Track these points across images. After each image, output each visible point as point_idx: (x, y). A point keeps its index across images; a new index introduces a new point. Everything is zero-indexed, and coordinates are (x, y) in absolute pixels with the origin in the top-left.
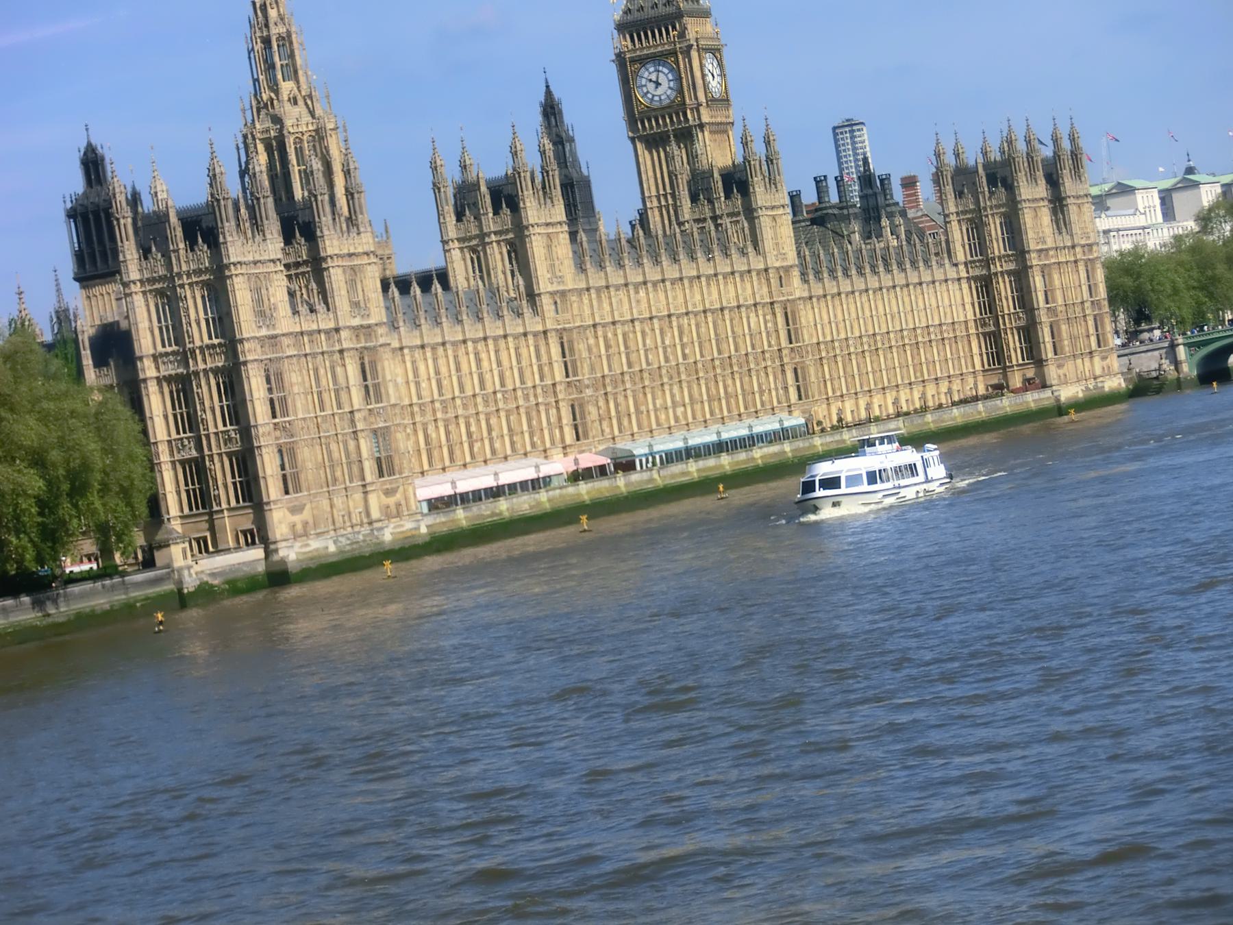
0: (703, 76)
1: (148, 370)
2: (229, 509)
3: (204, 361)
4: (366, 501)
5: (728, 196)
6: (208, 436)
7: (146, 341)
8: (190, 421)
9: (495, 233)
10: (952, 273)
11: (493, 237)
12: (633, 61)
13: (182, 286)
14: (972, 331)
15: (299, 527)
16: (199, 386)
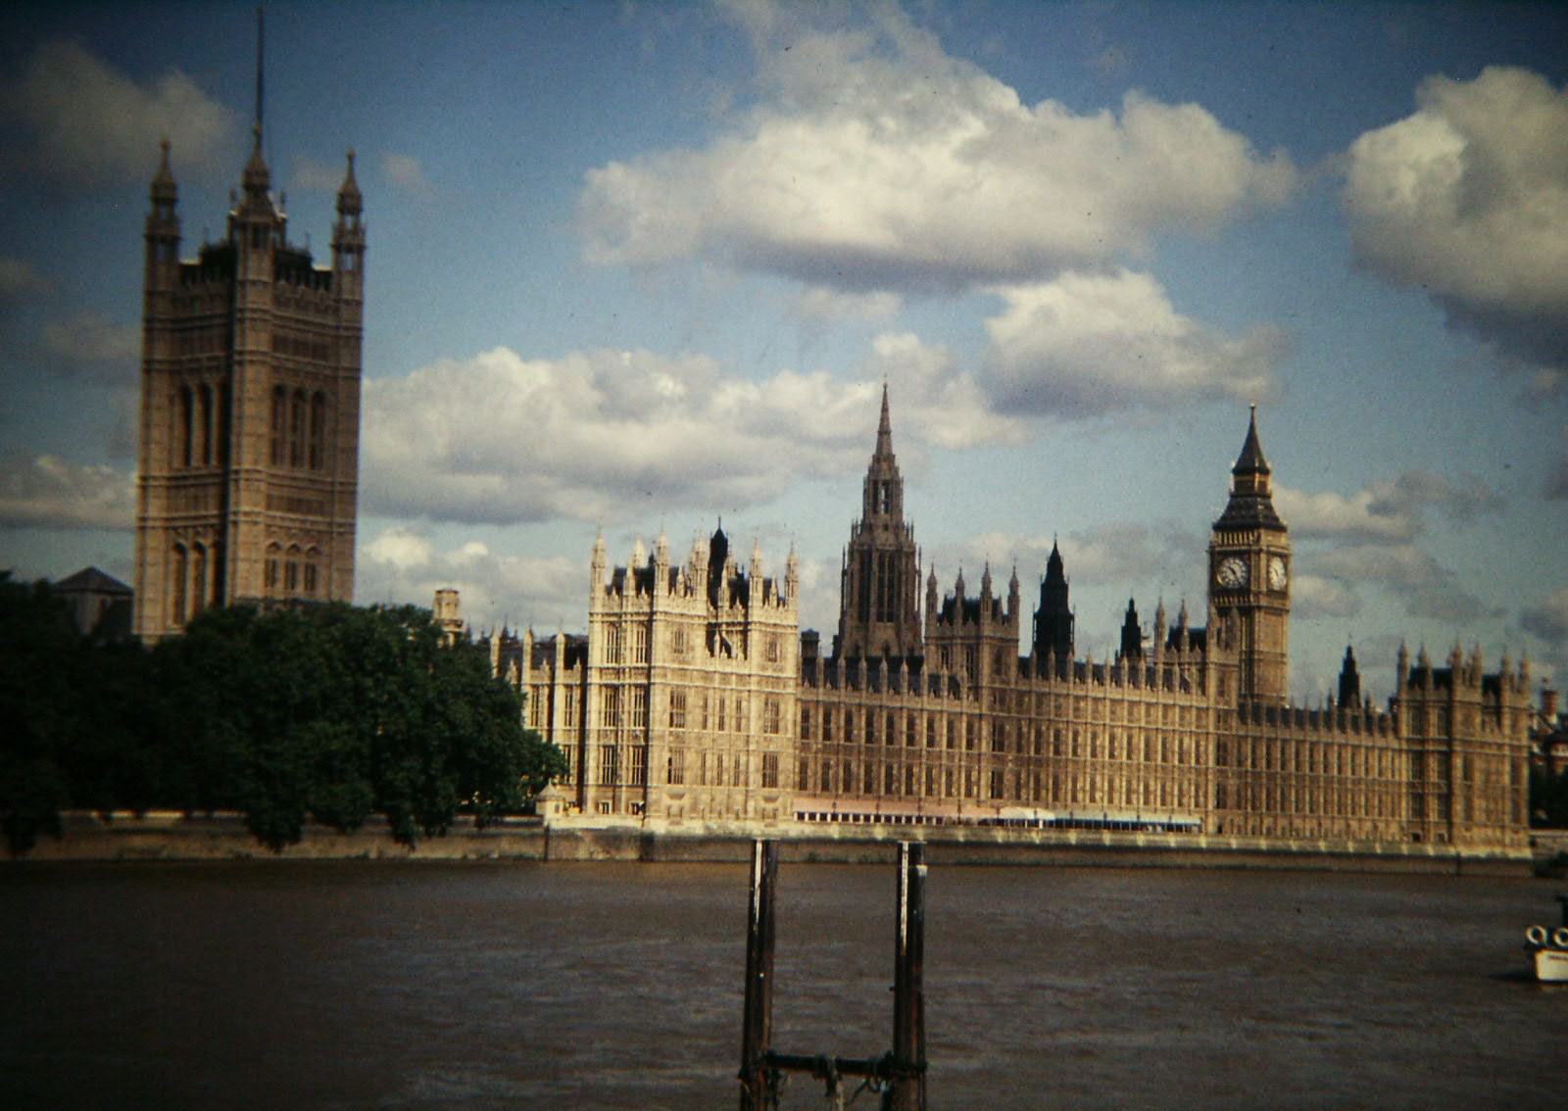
0: (1268, 572)
1: (594, 678)
2: (628, 786)
3: (630, 677)
4: (746, 802)
5: (965, 622)
6: (623, 731)
7: (597, 656)
8: (613, 718)
9: (961, 638)
10: (1395, 745)
11: (959, 641)
12: (1219, 553)
13: (626, 622)
14: (1404, 790)
15: (674, 810)
16: (623, 694)
